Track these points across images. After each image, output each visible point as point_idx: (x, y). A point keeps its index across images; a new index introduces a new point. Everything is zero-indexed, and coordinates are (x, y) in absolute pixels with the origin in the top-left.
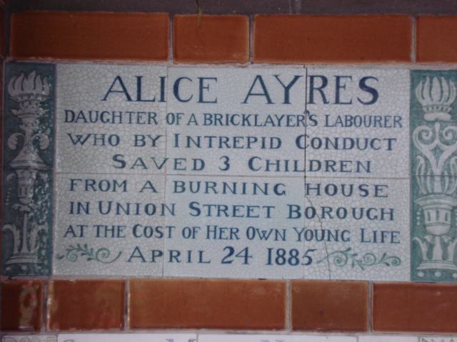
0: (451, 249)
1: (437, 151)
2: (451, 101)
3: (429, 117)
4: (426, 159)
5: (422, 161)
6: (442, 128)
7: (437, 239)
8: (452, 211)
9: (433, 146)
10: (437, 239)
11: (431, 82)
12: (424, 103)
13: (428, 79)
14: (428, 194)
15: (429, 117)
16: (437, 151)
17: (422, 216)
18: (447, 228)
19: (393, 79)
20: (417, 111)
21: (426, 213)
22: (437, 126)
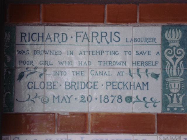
0: (181, 99)
1: (175, 59)
2: (179, 39)
3: (171, 45)
4: (170, 63)
5: (169, 63)
6: (176, 50)
7: (175, 95)
8: (181, 83)
9: (173, 57)
10: (175, 95)
11: (171, 32)
12: (169, 39)
13: (170, 31)
14: (171, 77)
15: (171, 45)
16: (175, 59)
17: (168, 85)
18: (178, 91)
19: (153, 31)
20: (165, 44)
21: (170, 84)
22: (174, 48)
